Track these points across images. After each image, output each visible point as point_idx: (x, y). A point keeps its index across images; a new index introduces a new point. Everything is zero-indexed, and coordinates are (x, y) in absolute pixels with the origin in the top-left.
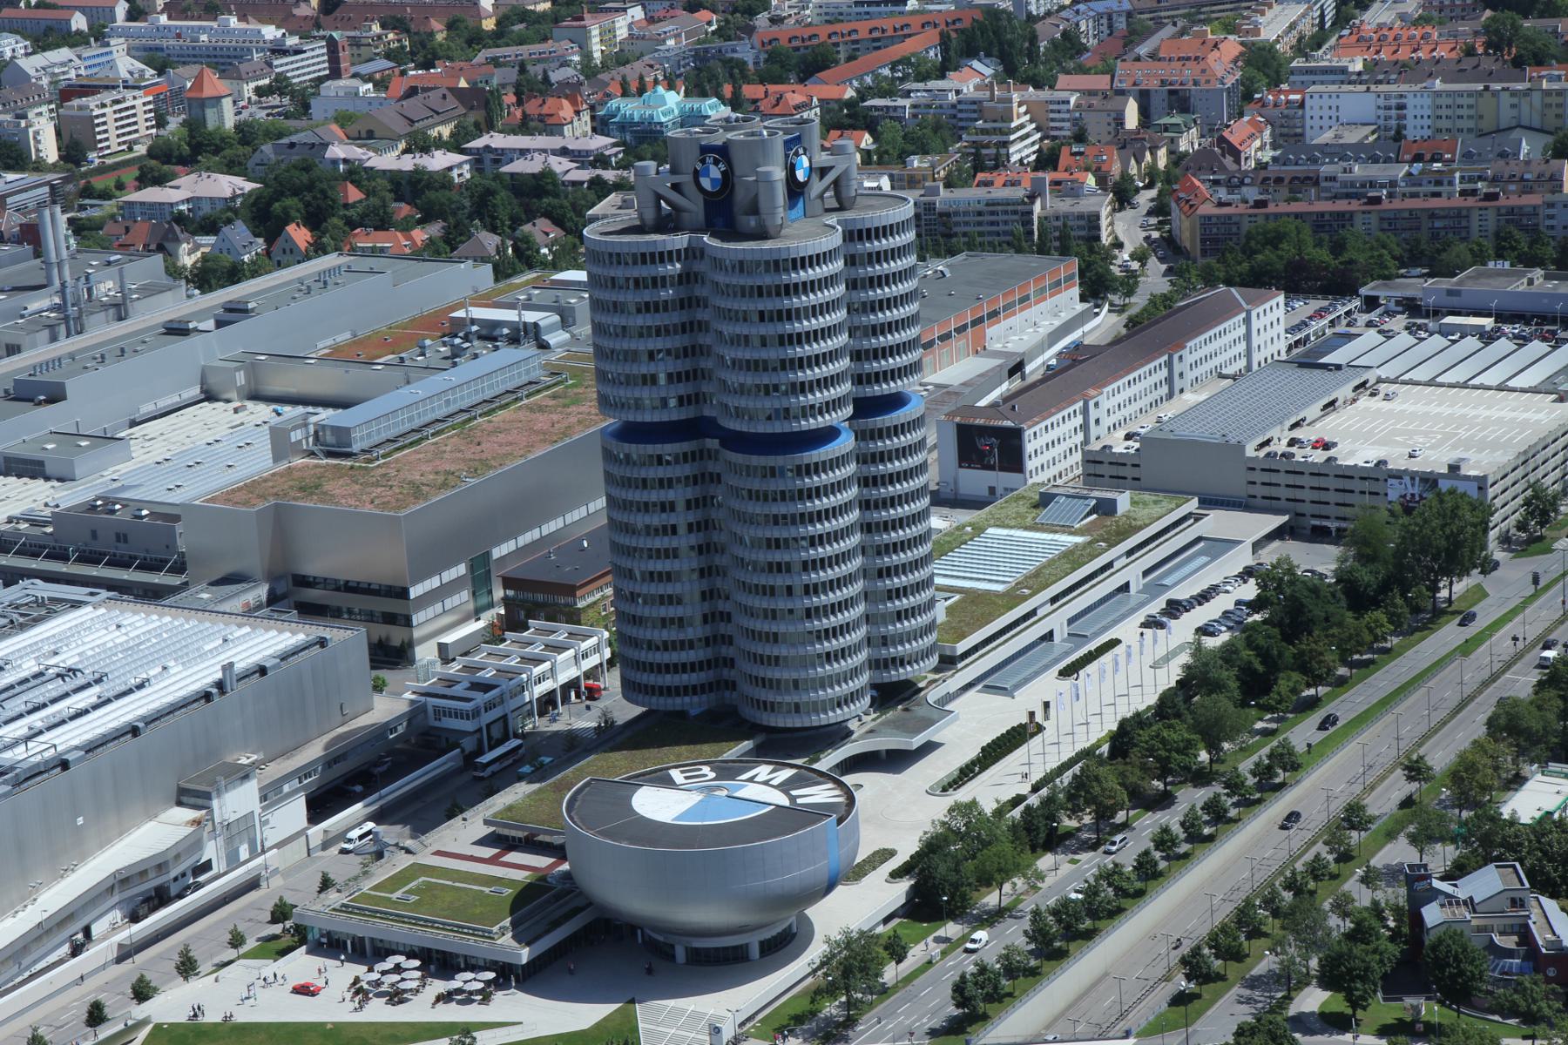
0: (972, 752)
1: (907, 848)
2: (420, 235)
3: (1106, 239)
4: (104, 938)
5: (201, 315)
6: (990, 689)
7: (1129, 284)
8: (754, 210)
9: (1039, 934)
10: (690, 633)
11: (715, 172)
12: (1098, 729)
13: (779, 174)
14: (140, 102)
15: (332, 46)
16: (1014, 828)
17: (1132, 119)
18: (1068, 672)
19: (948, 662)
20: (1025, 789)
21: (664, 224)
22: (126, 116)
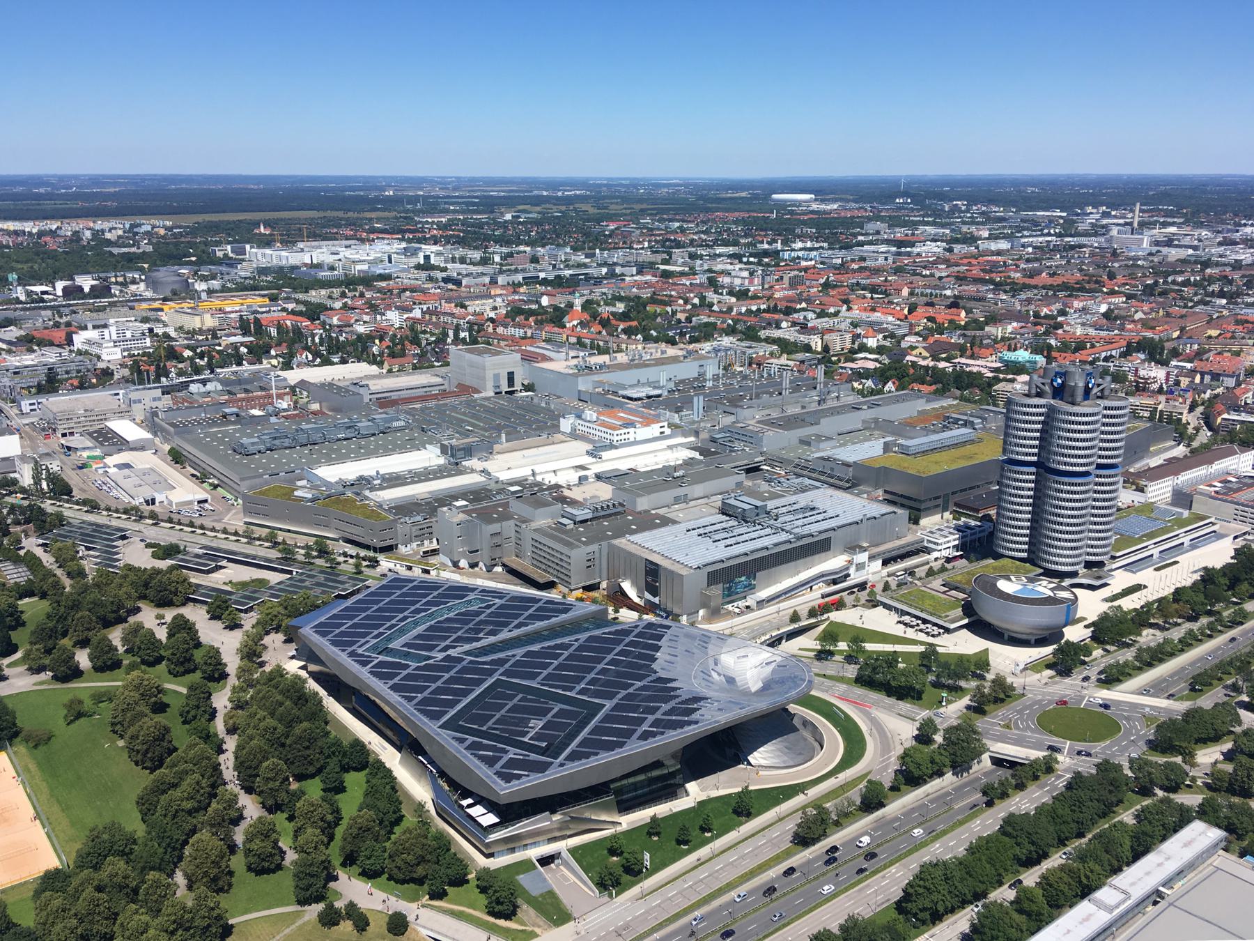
0: (1118, 590)
1: (1092, 618)
2: (934, 387)
3: (1184, 421)
4: (816, 590)
5: (864, 403)
6: (1126, 570)
7: (1191, 438)
8: (1073, 396)
9: (1137, 658)
10: (1022, 531)
11: (1059, 381)
12: (1168, 591)
13: (1081, 384)
14: (848, 337)
15: (911, 325)
16: (1132, 619)
17: (1198, 379)
18: (1155, 569)
19: (1113, 558)
20: (1138, 607)
21: (1040, 395)
22: (843, 340)
